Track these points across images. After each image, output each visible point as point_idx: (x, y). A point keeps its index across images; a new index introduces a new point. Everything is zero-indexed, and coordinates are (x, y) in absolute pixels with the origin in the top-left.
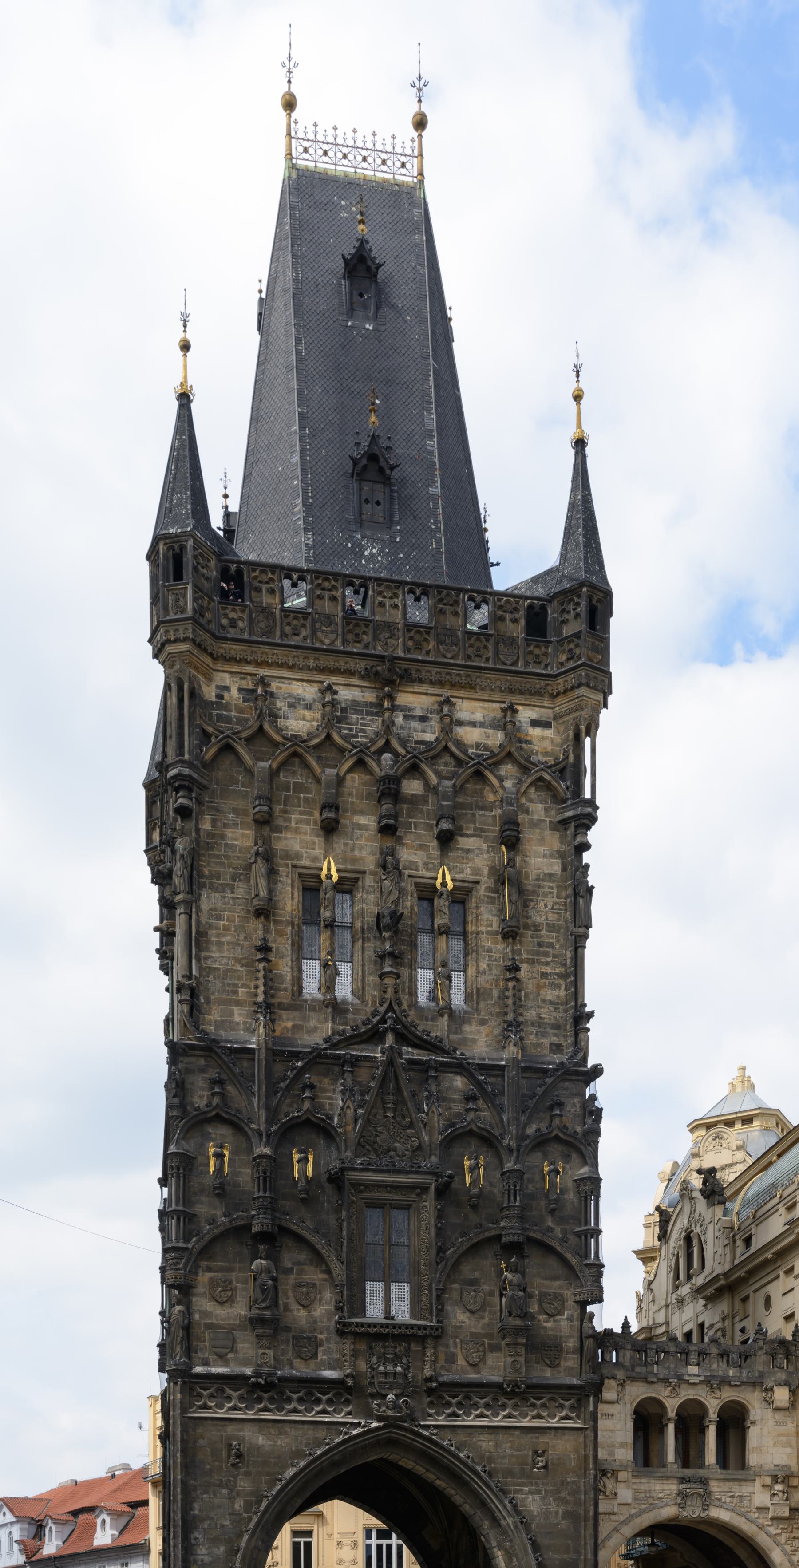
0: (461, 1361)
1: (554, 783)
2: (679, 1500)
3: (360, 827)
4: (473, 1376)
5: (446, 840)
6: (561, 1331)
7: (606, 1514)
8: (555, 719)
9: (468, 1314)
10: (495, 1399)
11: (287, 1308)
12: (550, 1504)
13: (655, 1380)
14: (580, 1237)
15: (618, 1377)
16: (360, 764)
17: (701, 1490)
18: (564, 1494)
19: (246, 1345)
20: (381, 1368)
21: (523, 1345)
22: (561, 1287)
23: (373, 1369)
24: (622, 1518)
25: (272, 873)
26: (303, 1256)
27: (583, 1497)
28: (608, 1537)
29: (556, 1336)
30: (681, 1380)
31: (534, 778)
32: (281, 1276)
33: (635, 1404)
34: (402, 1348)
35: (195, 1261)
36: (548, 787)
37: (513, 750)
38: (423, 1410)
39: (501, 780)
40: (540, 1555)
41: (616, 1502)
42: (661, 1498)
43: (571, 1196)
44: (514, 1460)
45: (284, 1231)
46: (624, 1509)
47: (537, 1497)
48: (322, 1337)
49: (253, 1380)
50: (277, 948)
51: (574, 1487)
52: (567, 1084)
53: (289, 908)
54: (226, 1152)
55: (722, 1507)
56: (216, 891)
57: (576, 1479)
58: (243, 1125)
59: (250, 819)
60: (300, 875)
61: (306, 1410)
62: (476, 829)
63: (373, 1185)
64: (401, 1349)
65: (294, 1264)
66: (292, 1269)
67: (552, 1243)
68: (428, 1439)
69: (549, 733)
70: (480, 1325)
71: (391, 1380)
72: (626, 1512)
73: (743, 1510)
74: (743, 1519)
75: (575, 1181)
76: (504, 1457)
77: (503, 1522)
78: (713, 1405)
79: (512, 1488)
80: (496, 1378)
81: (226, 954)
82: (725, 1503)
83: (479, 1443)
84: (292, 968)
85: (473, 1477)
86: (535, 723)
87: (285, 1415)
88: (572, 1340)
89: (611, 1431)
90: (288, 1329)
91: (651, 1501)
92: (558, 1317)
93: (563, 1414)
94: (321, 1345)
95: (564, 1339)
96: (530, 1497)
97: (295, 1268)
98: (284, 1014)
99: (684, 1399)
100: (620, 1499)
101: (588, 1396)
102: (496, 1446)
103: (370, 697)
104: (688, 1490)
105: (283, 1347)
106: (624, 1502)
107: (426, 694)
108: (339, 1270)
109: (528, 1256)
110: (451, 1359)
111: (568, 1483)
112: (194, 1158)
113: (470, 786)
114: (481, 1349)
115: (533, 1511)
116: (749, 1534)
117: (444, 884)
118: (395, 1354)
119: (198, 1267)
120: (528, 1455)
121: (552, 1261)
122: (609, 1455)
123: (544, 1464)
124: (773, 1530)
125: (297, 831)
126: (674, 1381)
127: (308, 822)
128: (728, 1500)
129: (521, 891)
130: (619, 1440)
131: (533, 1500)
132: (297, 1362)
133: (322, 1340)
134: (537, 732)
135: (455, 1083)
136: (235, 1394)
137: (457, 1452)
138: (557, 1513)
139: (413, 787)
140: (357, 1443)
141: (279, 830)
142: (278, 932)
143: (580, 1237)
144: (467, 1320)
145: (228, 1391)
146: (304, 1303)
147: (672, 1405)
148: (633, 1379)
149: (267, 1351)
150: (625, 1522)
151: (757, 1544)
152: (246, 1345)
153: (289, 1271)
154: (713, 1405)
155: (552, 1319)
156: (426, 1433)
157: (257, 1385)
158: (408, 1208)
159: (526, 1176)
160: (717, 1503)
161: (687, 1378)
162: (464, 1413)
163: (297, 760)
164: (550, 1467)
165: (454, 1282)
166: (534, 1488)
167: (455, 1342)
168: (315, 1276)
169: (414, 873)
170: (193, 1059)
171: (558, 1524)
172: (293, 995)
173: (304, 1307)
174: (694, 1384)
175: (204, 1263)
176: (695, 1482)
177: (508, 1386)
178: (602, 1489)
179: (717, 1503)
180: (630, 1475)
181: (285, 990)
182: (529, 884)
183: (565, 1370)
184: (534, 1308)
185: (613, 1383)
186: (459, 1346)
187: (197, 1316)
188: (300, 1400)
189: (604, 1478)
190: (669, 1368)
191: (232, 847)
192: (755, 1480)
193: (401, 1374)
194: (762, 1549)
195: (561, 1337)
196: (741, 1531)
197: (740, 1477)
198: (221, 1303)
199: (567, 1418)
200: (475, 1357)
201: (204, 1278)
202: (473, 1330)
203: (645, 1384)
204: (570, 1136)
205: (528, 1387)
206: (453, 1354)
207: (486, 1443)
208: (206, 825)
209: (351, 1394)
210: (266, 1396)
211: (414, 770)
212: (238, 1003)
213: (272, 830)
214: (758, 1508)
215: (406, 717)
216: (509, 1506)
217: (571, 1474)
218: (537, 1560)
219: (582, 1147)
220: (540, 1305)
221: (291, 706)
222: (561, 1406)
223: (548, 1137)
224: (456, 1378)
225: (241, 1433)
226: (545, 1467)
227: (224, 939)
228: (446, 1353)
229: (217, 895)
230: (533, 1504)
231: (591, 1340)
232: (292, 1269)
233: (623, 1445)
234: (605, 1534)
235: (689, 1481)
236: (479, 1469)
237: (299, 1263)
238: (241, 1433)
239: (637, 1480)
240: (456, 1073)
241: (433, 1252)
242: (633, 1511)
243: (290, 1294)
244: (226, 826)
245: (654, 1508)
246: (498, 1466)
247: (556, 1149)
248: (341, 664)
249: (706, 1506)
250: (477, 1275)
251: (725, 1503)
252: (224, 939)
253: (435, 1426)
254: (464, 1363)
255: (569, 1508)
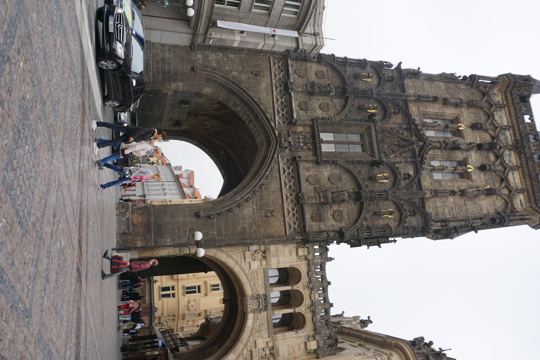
0: (308, 174)
1: (509, 208)
2: (255, 296)
3: (476, 138)
4: (303, 180)
5: (482, 168)
6: (327, 221)
7: (244, 255)
8: (524, 209)
9: (328, 177)
10: (294, 191)
11: (318, 99)
12: (248, 220)
13: (310, 276)
14: (367, 228)
15: (309, 256)
16: (493, 138)
17: (261, 307)
18: (254, 227)
19: (301, 82)
20: (301, 137)
21: (320, 201)
22: (345, 220)
23: (300, 134)
24: (243, 265)
25: (456, 105)
26: (338, 108)
27: (254, 237)
28: (233, 259)
29: (324, 219)
30: (312, 289)
31: (508, 200)
32: (329, 98)
33: (297, 267)
34: (310, 146)
35: (330, 64)
36: (506, 207)
37: (513, 192)
38: (285, 157)
39: (503, 188)
40: (223, 215)
41: (250, 260)
42: (255, 286)
43: (381, 222)
44: (268, 200)
45: (347, 99)
46: (247, 266)
47: (251, 213)
48: (309, 113)
49: (289, 82)
50: (435, 107)
51: (258, 232)
52: (420, 219)
53: (448, 112)
54: (369, 80)
55: (254, 320)
56: (446, 88)
57: (262, 233)
58: (380, 86)
59: (468, 101)
60: (457, 117)
61: (279, 105)
62: (487, 180)
63: (370, 135)
64: (310, 146)
65: (335, 104)
66: (333, 103)
67: (363, 214)
68: (273, 158)
69: (520, 207)
70: (324, 183)
71: (296, 140)
72: (246, 267)
73: (254, 333)
74: (249, 334)
75: (387, 224)
76: (268, 195)
77: (238, 196)
78: (302, 309)
79: (255, 200)
80: (304, 190)
81: (429, 89)
82: (256, 322)
83: (273, 183)
84: (430, 112)
85: (258, 180)
86: (520, 201)
87: (276, 96)
88: (324, 227)
89: (284, 255)
90: (310, 100)
91: (253, 280)
92: (333, 219)
93: (292, 225)
94: (306, 113)
95: (324, 223)
96: (251, 209)
97: (334, 104)
98: (416, 108)
99: (303, 292)
100: (252, 263)
101: (302, 236)
102: (273, 192)
103: (510, 143)
104: (261, 299)
105: (303, 97)
106: (251, 265)
107: (517, 162)
108: (338, 119)
109: (355, 204)
110: (308, 169)
111: (260, 229)
112: (365, 70)
113: (498, 178)
114: (315, 182)
115: (244, 211)
116: (242, 339)
117: (469, 168)
118: (307, 143)
119: (327, 67)
120: (270, 207)
121: (354, 216)
122: (273, 255)
123: (268, 216)
124: (245, 352)
125: (469, 116)
126: (311, 286)
127: (472, 120)
128: (258, 324)
129: (476, 196)
130: (280, 259)
131: (250, 211)
132: (297, 102)
133: (308, 113)
134: (519, 203)
135: (411, 171)
136: (281, 76)
137: (269, 171)
138: (245, 224)
139: (492, 157)
140: (267, 125)
141: (468, 110)
142: (440, 107)
143: (367, 228)
144: (325, 177)
145: (282, 74)
146: (321, 106)
147: (299, 287)
148: (309, 265)
149: (301, 88)
150: (241, 268)
151: (237, 344)
152: (300, 81)
153: (332, 102)
154: (302, 309)
155: (332, 217)
156: (276, 156)
157: (287, 83)
158: (363, 150)
159: (385, 202)
160: (256, 318)
161: (313, 292)
162: (286, 176)
163: (487, 117)
164: (266, 219)
165: (339, 170)
166: (256, 211)
167: (315, 171)
168: (332, 113)
169: (469, 157)
170: (396, 73)
171: (239, 224)
172: (423, 112)
173: (320, 107)
174: (311, 297)
175: (329, 69)
176: (265, 303)
177: (301, 195)
178: (257, 252)
179: (256, 318)
180: (265, 267)
181: (424, 109)
182: (477, 200)
183: (311, 224)
184: (335, 207)
185: (306, 253)
186: (314, 173)
187: (309, 64)
188: (282, 103)
189: (262, 253)
190: (316, 283)
191: (458, 94)
192: (269, 337)
193: (300, 146)
194: (235, 347)
195: (325, 221)
196: (242, 334)
197: (270, 328)
198: (316, 74)
199: (290, 227)
200: (311, 180)
201: (324, 69)
202: (321, 180)
203: (307, 271)
204: (404, 220)
205: (302, 204)
206: (310, 170)
207: (274, 186)
208: (462, 86)
209: (287, 124)
210: (282, 88)
211: (497, 157)
212: (415, 92)
213: (467, 108)
214: (255, 341)
215: (509, 155)
216: (247, 197)
217: (264, 230)
218: (221, 213)
219: (401, 226)
220: (336, 211)
221: (500, 116)
222: (295, 223)
223: (402, 210)
224: (301, 171)
225: (265, 77)
226: (266, 216)
227: (433, 89)
228: (310, 167)
229: (444, 88)
230: (248, 210)
231: (327, 236)
232: (333, 103)
233: (278, 262)
234: (234, 257)
235: (265, 300)
236: (262, 181)
237: (335, 106)
238: (265, 77)
239: (262, 272)
240: (414, 171)
241: (351, 160)
242: (247, 271)
243: (324, 101)
244: (464, 93)
245: (249, 282)
246: (264, 193)
247: (396, 215)
248: (517, 132)
249: (253, 311)
250: (344, 181)
251: (256, 322)
252: (433, 89)
253: (279, 160)
254: (307, 176)
255: (248, 230)
